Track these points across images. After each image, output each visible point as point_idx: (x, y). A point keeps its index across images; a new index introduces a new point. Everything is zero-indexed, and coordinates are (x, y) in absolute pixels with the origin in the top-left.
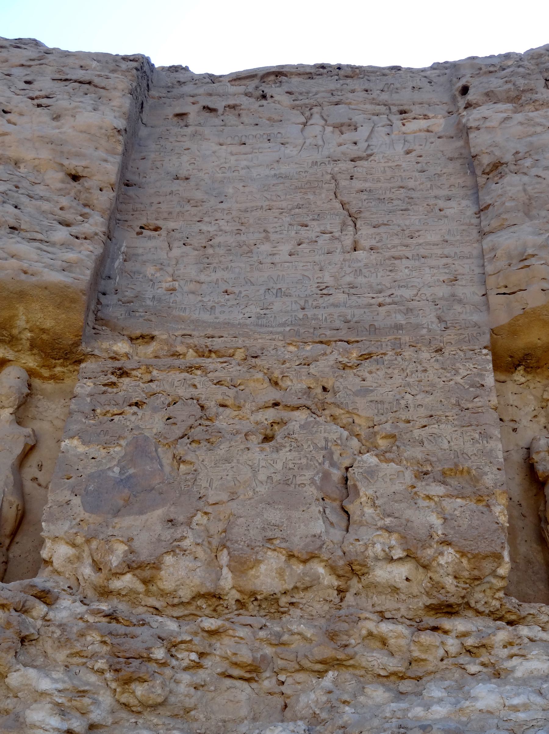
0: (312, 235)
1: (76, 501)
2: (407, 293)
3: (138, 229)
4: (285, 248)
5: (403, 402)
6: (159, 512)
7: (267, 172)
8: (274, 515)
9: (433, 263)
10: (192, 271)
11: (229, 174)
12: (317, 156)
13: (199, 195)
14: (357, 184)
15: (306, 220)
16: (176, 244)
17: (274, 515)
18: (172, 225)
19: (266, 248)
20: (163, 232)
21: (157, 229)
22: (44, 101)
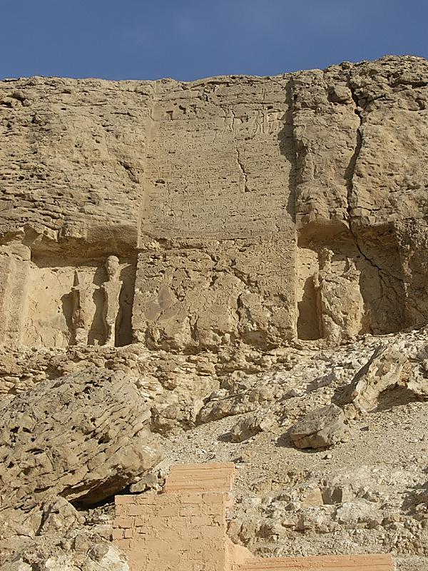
0: (228, 184)
1: (143, 314)
2: (265, 214)
3: (155, 183)
4: (217, 192)
5: (261, 266)
6: (173, 317)
7: (208, 147)
8: (213, 317)
9: (276, 197)
10: (179, 204)
11: (192, 150)
12: (231, 137)
13: (180, 162)
14: (247, 154)
15: (224, 175)
16: (171, 191)
17: (213, 317)
18: (169, 180)
19: (208, 192)
20: (166, 184)
21: (163, 182)
22: (109, 128)
